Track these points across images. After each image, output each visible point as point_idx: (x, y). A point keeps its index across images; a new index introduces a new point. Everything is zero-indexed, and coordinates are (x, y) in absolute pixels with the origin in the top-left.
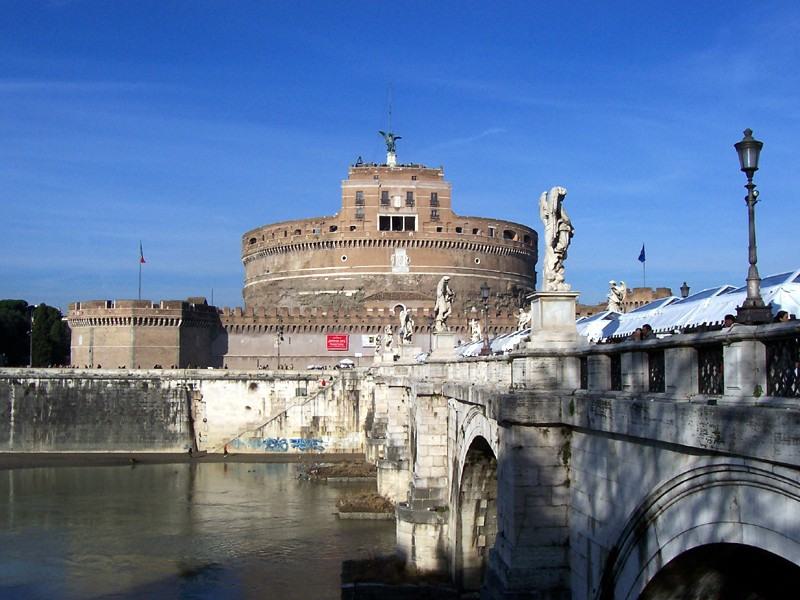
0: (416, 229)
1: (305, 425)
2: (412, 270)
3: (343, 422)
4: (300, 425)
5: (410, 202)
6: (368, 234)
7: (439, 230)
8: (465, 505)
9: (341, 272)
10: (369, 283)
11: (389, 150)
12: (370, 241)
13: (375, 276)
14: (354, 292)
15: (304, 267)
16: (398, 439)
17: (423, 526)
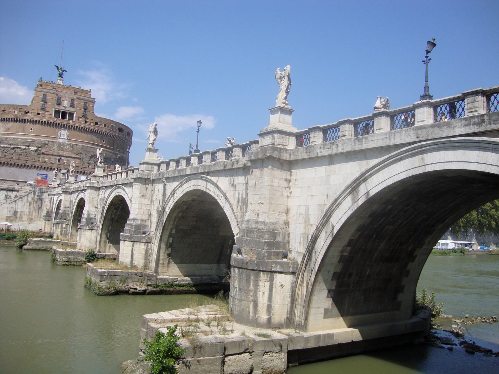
0: (74, 119)
1: (9, 215)
3: (32, 215)
4: (6, 215)
5: (72, 106)
7: (86, 122)
8: (165, 231)
9: (28, 137)
10: (44, 145)
11: (59, 77)
12: (48, 122)
13: (48, 141)
14: (36, 148)
15: (6, 131)
16: (92, 214)
17: (138, 243)
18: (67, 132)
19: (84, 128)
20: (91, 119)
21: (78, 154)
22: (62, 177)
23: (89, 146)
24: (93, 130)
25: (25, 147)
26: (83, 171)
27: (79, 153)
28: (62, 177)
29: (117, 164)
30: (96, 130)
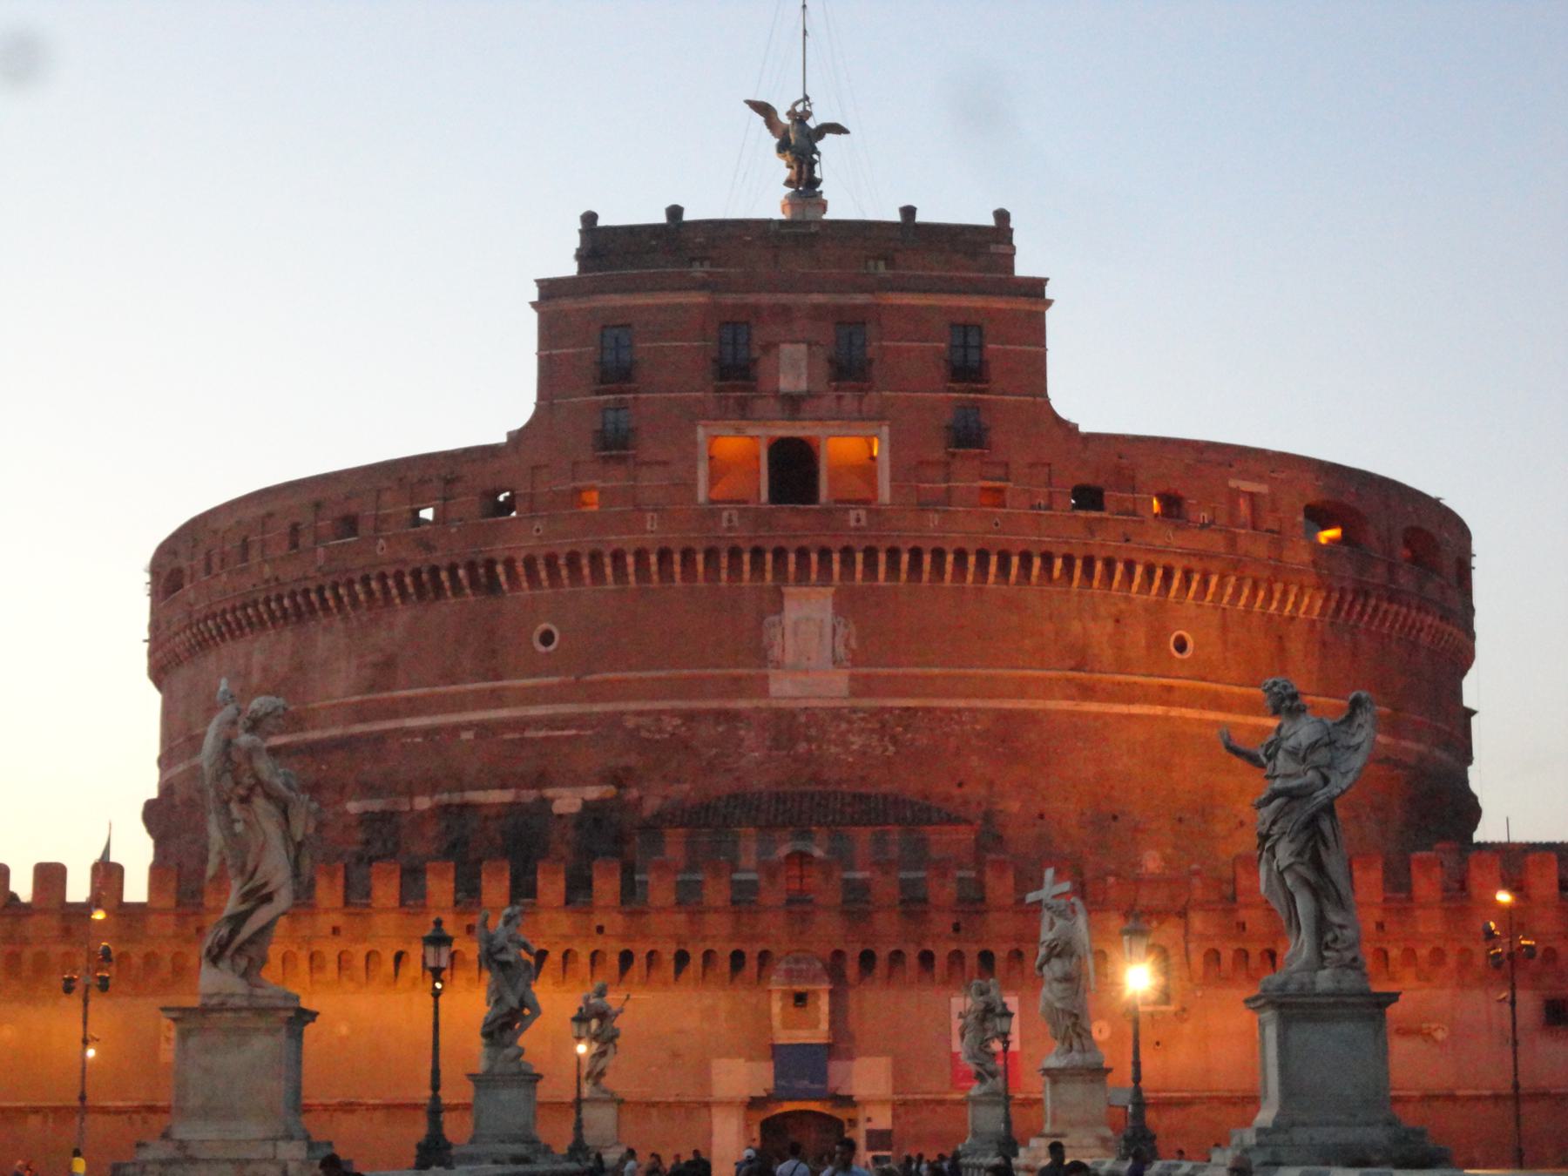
0: (885, 493)
2: (862, 686)
6: (651, 523)
12: (664, 555)
13: (690, 717)
14: (593, 792)
15: (372, 687)
18: (839, 610)
19: (983, 557)
20: (1032, 465)
21: (956, 792)
22: (786, 1025)
23: (1052, 705)
24: (1069, 561)
25: (507, 796)
26: (972, 951)
27: (960, 785)
28: (786, 1025)
29: (1049, 873)
30: (1089, 563)
